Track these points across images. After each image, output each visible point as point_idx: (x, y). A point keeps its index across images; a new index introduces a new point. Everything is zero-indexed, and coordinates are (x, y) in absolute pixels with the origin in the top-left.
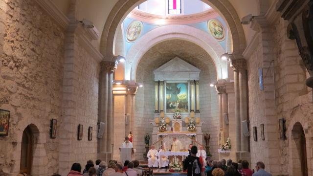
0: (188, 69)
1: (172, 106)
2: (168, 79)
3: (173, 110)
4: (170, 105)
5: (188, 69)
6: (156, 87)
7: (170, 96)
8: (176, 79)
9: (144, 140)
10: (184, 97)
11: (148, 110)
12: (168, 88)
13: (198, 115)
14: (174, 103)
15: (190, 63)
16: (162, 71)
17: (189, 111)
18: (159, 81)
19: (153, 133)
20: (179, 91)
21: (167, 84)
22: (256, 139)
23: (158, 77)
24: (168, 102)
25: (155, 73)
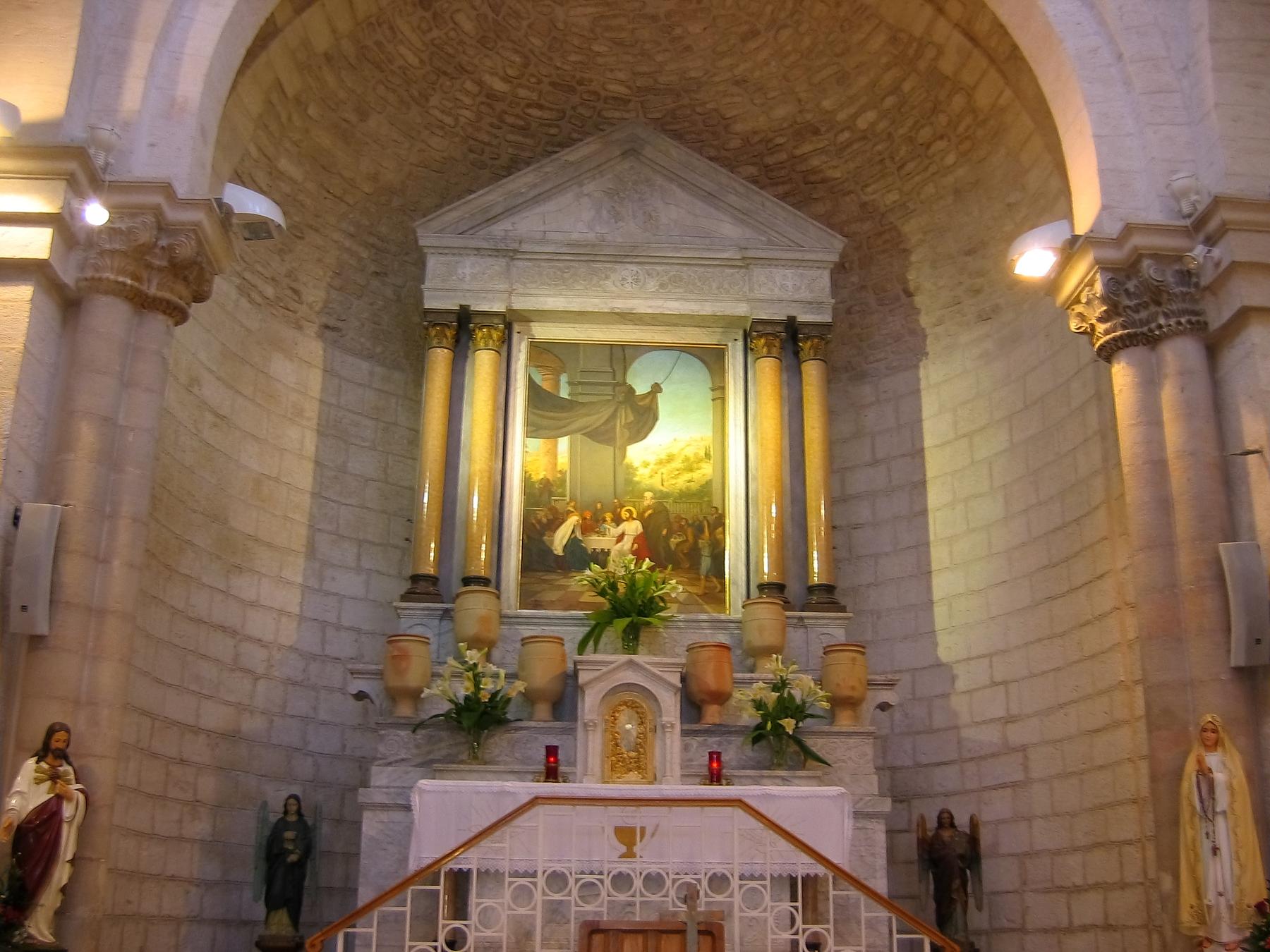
0: (730, 221)
1: (573, 544)
4: (560, 539)
5: (730, 221)
6: (440, 359)
7: (563, 460)
8: (620, 304)
11: (349, 583)
12: (546, 385)
13: (827, 628)
14: (591, 525)
16: (498, 229)
19: (363, 796)
21: (540, 351)
24: (542, 514)
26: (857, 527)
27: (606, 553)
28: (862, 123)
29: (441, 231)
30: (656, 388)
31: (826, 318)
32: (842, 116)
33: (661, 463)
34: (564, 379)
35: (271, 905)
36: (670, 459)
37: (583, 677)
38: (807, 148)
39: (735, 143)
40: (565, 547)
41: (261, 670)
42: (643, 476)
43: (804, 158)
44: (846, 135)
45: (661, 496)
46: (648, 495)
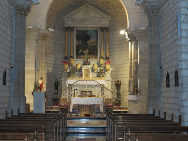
1: (81, 52)
2: (79, 26)
3: (82, 56)
4: (80, 52)
7: (80, 43)
9: (53, 86)
10: (94, 43)
12: (78, 34)
14: (83, 50)
15: (100, 10)
17: (99, 57)
18: (69, 28)
20: (88, 38)
21: (77, 31)
22: (168, 86)
23: (69, 23)
25: (65, 19)
26: (113, 48)
27: (85, 53)
28: (114, 2)
29: (66, 18)
30: (90, 34)
31: (109, 27)
32: (112, 1)
33: (91, 43)
34: (80, 34)
35: (55, 90)
36: (92, 42)
37: (82, 68)
38: (108, 4)
39: (100, 3)
40: (81, 53)
41: (50, 66)
42: (89, 44)
43: (108, 5)
44: (112, 3)
45: (90, 47)
46: (89, 47)
